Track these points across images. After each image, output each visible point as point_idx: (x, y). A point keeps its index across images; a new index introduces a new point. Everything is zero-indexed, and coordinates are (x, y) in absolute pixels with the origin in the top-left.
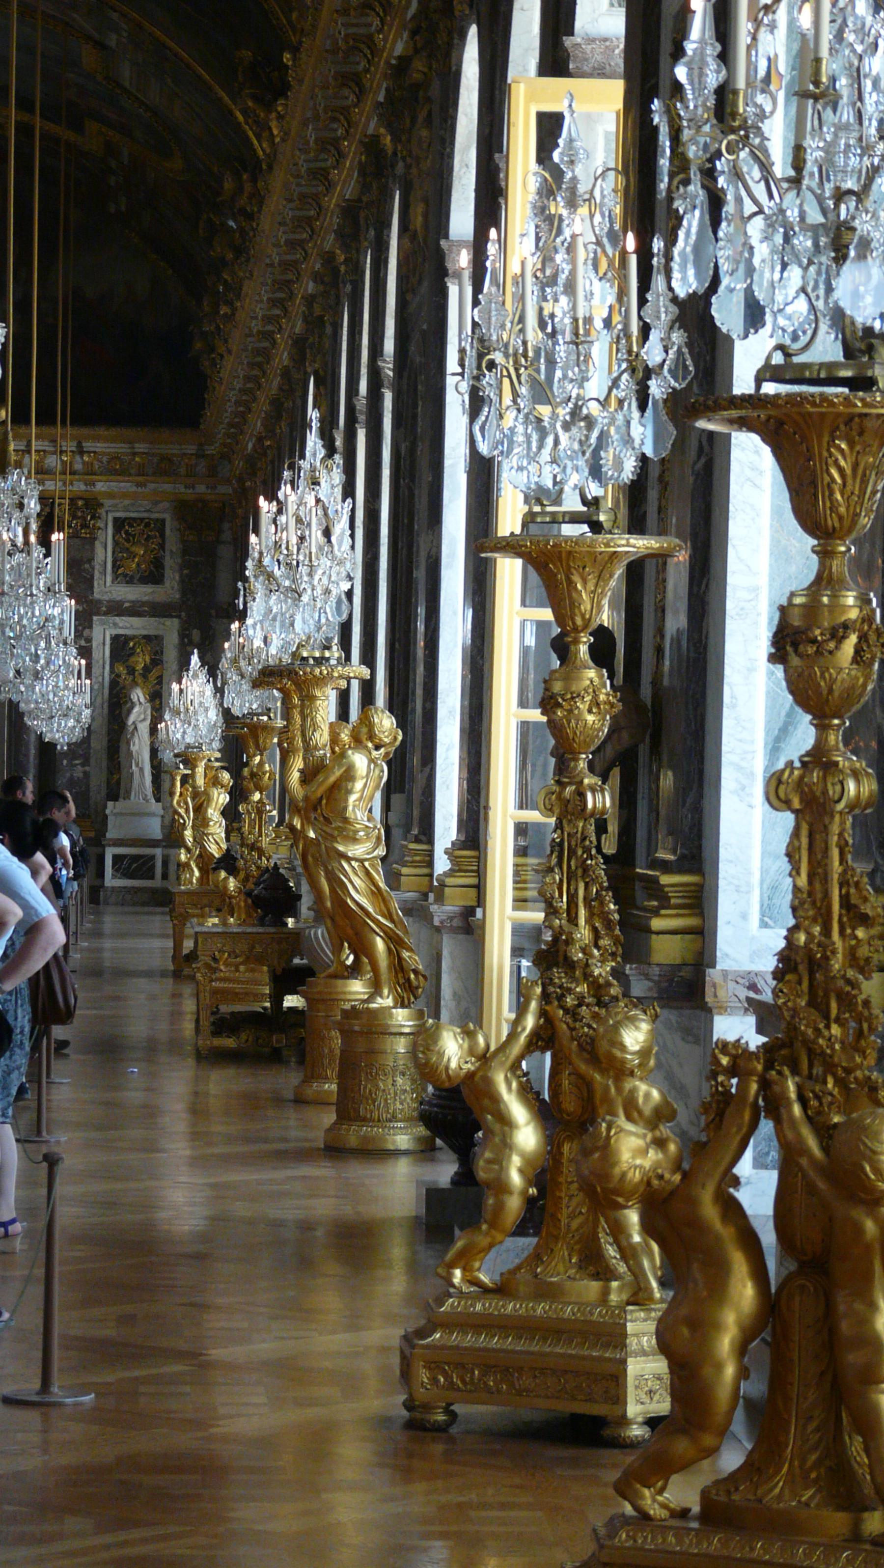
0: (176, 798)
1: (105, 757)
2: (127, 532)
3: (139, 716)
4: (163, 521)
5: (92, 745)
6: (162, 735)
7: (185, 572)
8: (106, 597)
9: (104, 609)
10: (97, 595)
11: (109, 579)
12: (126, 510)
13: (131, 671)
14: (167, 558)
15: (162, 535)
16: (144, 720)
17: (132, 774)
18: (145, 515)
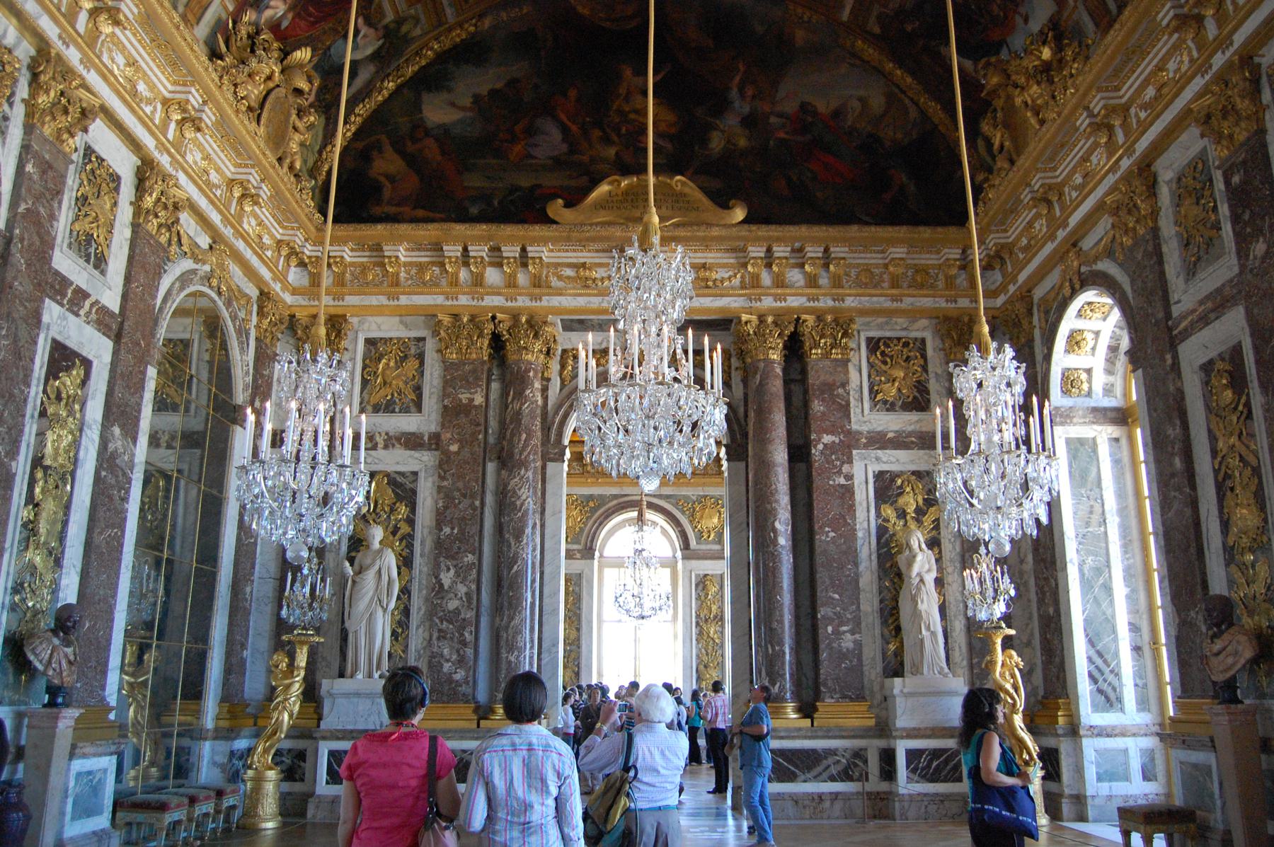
1: (878, 622)
2: (883, 353)
3: (922, 566)
4: (923, 341)
9: (864, 440)
10: (855, 427)
11: (867, 405)
12: (880, 327)
13: (902, 514)
15: (924, 357)
16: (929, 570)
17: (922, 641)
18: (903, 334)
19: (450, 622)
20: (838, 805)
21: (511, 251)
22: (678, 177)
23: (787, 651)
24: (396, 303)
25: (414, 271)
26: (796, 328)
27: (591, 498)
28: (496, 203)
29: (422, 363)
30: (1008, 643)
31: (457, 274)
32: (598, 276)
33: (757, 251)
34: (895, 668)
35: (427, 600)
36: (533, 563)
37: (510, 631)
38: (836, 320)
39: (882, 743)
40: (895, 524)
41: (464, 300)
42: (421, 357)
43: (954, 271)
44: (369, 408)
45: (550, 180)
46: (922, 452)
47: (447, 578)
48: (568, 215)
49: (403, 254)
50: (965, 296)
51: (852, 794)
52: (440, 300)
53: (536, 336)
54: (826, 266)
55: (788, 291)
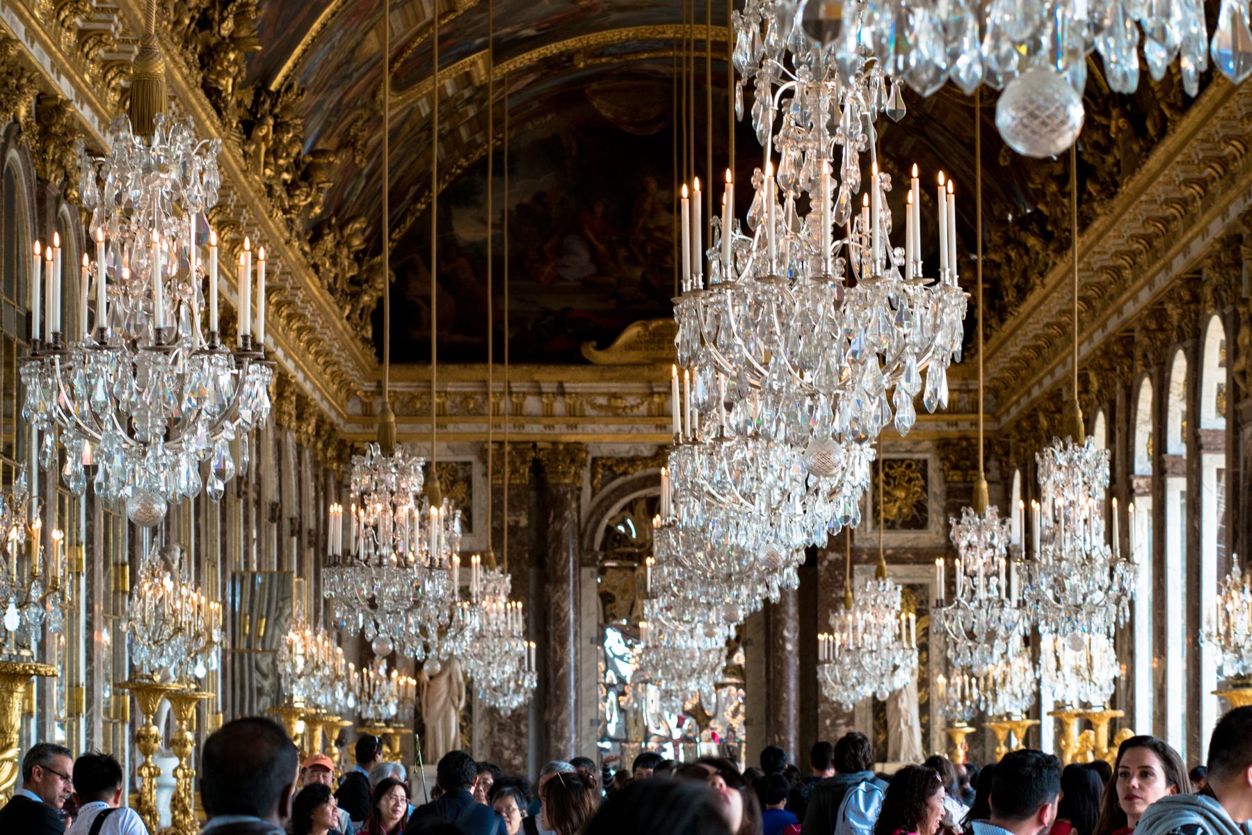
1: (870, 715)
4: (925, 462)
8: (867, 545)
9: (865, 557)
15: (925, 477)
21: (549, 387)
25: (458, 399)
28: (529, 327)
29: (470, 486)
37: (559, 724)
42: (468, 481)
45: (581, 304)
46: (916, 567)
53: (573, 461)
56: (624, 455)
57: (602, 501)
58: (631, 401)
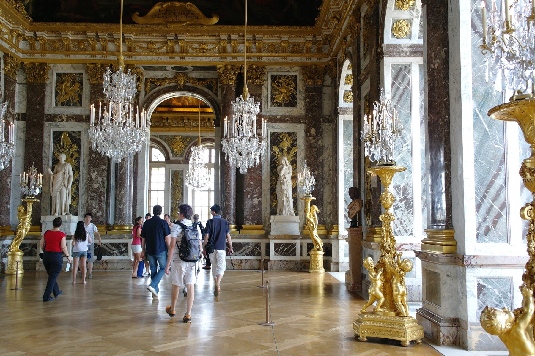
0: (308, 213)
1: (269, 193)
2: (278, 82)
3: (286, 172)
4: (296, 76)
5: (262, 187)
6: (299, 179)
7: (307, 100)
11: (269, 104)
13: (281, 150)
14: (298, 94)
16: (289, 173)
17: (283, 201)
18: (287, 73)
19: (95, 193)
20: (248, 264)
22: (188, 3)
23: (232, 204)
24: (69, 58)
25: (76, 43)
26: (241, 71)
27: (188, 137)
29: (82, 85)
30: (313, 203)
31: (95, 45)
32: (156, 47)
33: (224, 37)
34: (274, 212)
35: (86, 184)
36: (130, 169)
37: (120, 197)
38: (258, 67)
39: (266, 241)
40: (278, 154)
41: (98, 57)
42: (81, 82)
43: (310, 45)
44: (59, 104)
47: (94, 175)
48: (140, 20)
49: (70, 36)
50: (315, 57)
51: (254, 260)
52: (88, 57)
54: (255, 43)
55: (238, 54)
56: (160, 77)
57: (149, 97)
58: (158, 45)
